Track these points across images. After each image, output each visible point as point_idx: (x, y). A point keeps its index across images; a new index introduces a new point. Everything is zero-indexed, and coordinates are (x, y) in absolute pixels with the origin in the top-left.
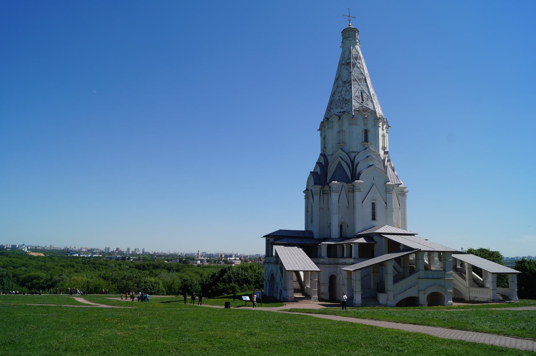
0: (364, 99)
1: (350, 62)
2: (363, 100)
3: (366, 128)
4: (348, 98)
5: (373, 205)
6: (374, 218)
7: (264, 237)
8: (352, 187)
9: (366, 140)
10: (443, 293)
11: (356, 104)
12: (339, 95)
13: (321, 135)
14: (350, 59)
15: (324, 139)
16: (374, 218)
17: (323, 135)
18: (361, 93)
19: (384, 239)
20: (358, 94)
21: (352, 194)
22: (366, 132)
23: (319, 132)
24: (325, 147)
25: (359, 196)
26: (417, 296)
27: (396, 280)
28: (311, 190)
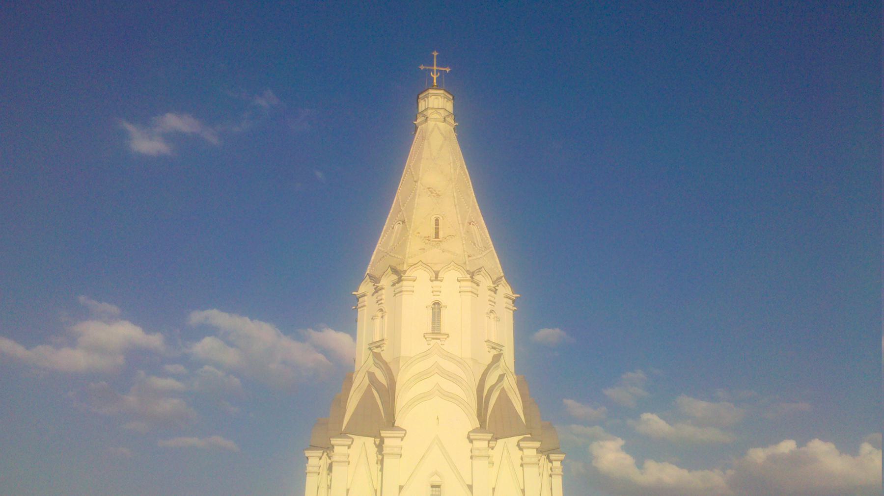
3: (436, 298)
18: (437, 221)
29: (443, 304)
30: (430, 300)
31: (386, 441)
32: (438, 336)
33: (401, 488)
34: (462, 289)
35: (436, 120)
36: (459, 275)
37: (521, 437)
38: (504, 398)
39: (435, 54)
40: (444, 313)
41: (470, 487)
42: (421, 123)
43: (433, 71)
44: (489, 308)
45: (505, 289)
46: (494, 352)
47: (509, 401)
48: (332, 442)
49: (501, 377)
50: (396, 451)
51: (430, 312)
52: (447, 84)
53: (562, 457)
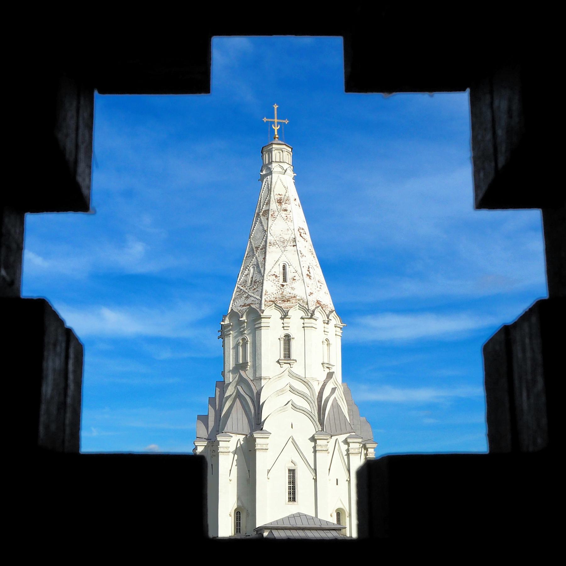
0: (289, 276)
1: (268, 210)
2: (285, 280)
3: (287, 332)
4: (258, 278)
5: (292, 472)
6: (292, 498)
9: (288, 355)
11: (270, 287)
12: (246, 272)
14: (268, 203)
16: (292, 498)
18: (284, 268)
20: (278, 270)
22: (288, 339)
25: (262, 461)
30: (282, 333)
31: (258, 441)
32: (289, 362)
33: (269, 471)
34: (305, 325)
35: (280, 173)
36: (303, 314)
37: (349, 434)
38: (336, 406)
39: (276, 107)
40: (293, 343)
41: (315, 470)
42: (266, 175)
43: (273, 122)
44: (325, 337)
45: (335, 320)
46: (327, 371)
47: (338, 406)
48: (218, 439)
49: (334, 390)
50: (264, 447)
51: (282, 342)
52: (287, 137)
53: (375, 445)
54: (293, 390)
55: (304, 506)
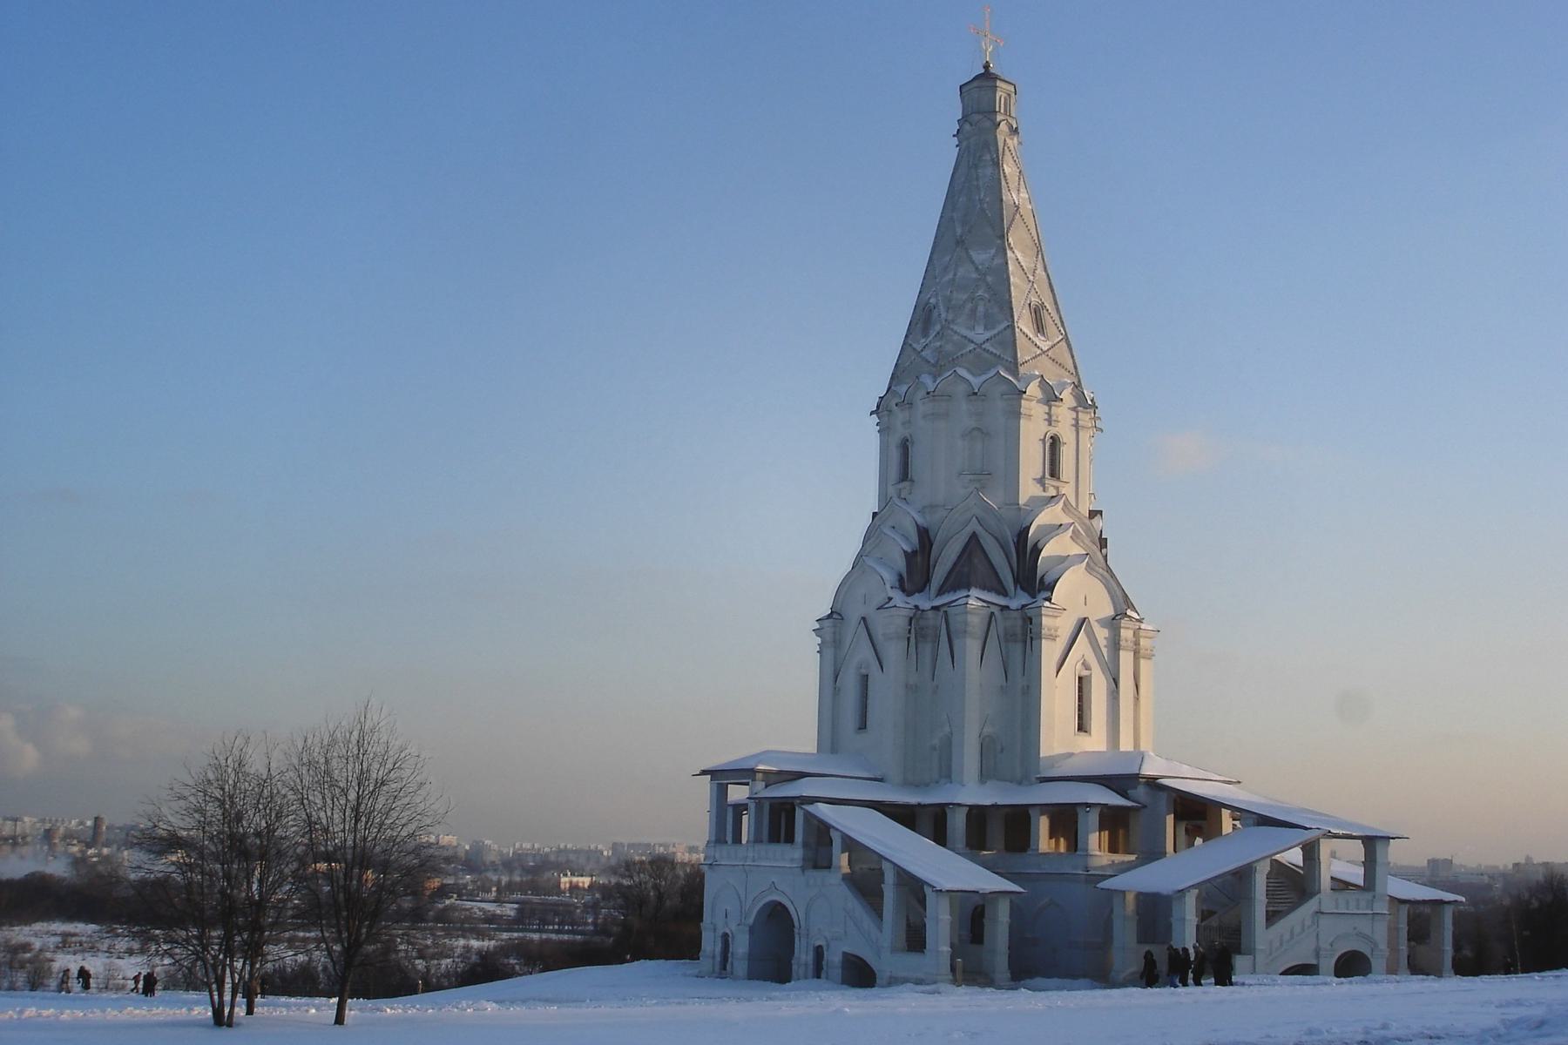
3: (1053, 431)
6: (1082, 727)
7: (704, 772)
8: (1020, 622)
10: (1367, 952)
13: (884, 430)
15: (905, 446)
16: (1082, 727)
17: (900, 432)
19: (1164, 795)
21: (1018, 647)
22: (1055, 443)
23: (875, 418)
24: (905, 475)
26: (1314, 962)
27: (1272, 917)
28: (864, 619)
29: (1064, 439)
54: (1075, 537)
55: (1096, 741)
